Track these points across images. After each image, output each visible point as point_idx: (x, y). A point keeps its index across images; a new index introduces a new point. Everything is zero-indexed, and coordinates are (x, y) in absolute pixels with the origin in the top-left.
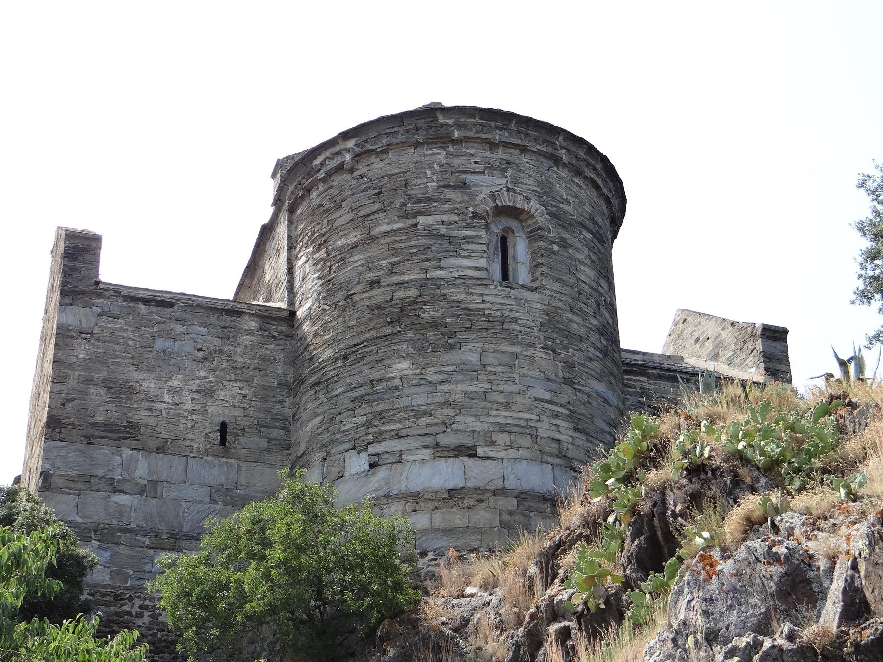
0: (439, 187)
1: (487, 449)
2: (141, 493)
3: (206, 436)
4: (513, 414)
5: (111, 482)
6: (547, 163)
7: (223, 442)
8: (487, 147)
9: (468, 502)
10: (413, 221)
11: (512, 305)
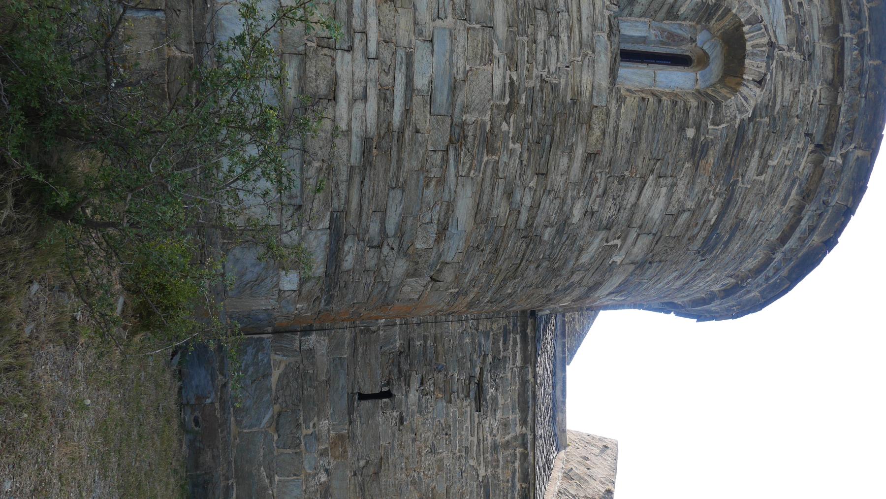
6: (818, 131)
8: (829, 22)
11: (580, 32)
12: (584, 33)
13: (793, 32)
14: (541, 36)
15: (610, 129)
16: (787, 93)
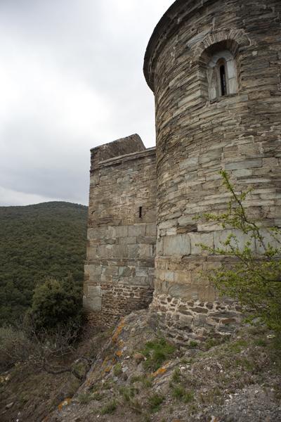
0: (176, 59)
1: (203, 225)
2: (115, 243)
3: (134, 215)
4: (221, 196)
5: (106, 241)
7: (140, 215)
9: (191, 266)
10: (166, 89)
12: (218, 112)
13: (205, 26)
14: (223, 128)
15: (258, 89)
16: (230, 17)
